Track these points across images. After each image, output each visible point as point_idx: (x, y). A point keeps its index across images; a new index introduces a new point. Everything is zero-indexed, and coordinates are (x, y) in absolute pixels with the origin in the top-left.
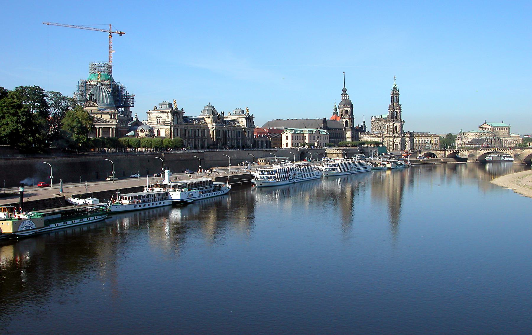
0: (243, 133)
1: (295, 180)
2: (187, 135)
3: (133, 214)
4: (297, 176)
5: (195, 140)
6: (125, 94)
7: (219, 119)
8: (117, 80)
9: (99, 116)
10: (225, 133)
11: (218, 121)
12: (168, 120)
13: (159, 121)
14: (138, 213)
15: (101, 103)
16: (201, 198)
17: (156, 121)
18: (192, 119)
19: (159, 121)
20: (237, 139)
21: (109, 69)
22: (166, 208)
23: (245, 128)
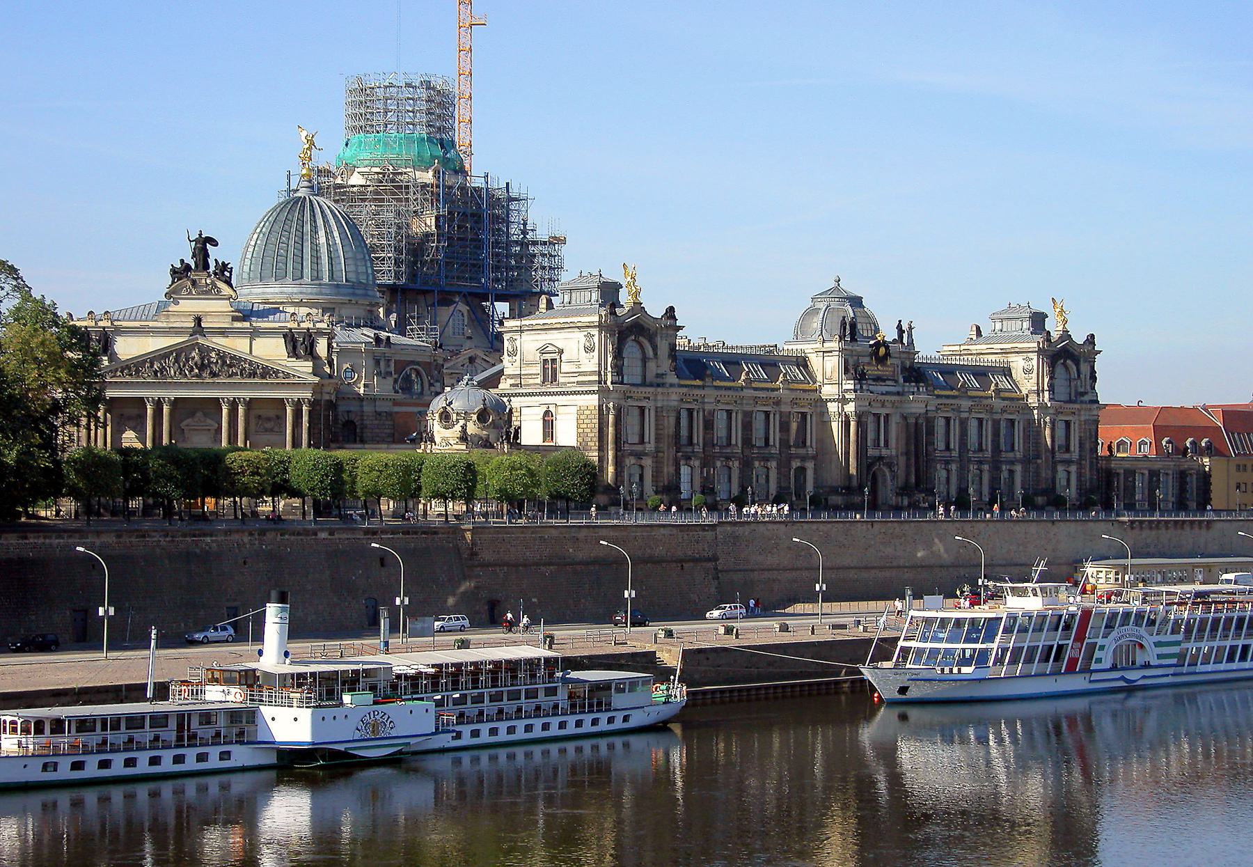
0: (1033, 431)
1: (1132, 675)
2: (698, 437)
3: (36, 800)
4: (1150, 655)
5: (746, 465)
6: (514, 230)
7: (882, 360)
8: (489, 162)
9: (238, 345)
10: (918, 434)
11: (873, 370)
12: (590, 363)
13: (550, 370)
14: (64, 799)
15: (307, 279)
16: (446, 741)
17: (537, 369)
18: (733, 361)
19: (550, 370)
20: (996, 466)
21: (439, 107)
22: (240, 784)
23: (1043, 407)
